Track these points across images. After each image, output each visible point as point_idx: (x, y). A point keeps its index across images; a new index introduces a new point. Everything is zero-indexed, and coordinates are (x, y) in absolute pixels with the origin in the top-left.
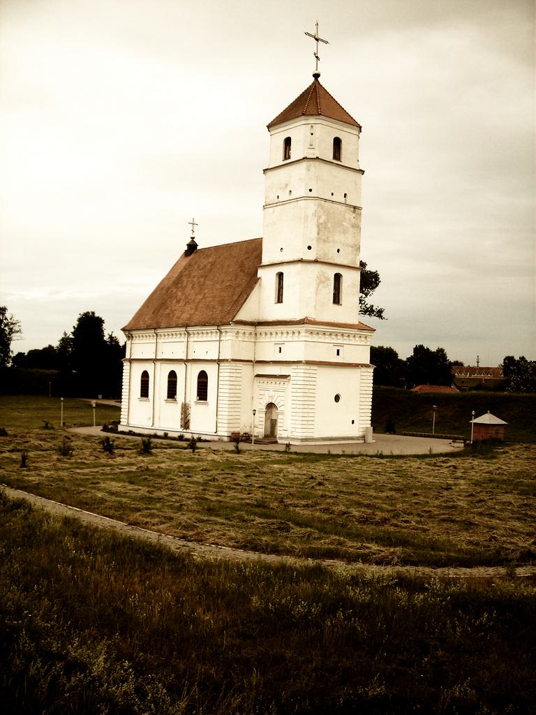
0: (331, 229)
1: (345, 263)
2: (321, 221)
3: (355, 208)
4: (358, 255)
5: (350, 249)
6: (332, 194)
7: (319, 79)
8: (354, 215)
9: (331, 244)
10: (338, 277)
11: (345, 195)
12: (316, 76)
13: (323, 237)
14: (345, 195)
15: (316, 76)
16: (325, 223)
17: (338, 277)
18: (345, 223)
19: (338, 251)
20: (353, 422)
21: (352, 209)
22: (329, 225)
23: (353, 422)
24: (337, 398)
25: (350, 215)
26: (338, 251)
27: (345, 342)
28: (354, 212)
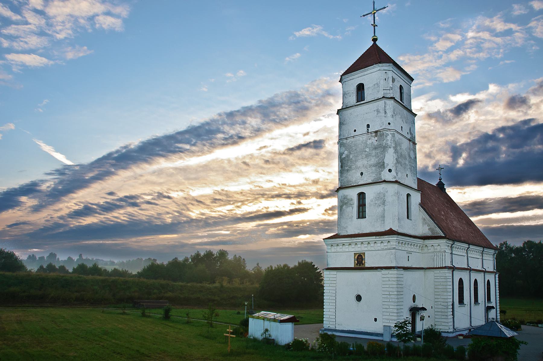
0: (354, 159)
1: (370, 181)
2: (344, 156)
3: (376, 132)
4: (382, 171)
5: (374, 168)
6: (355, 131)
7: (377, 42)
8: (376, 138)
9: (354, 171)
10: (362, 196)
11: (368, 126)
12: (375, 40)
13: (346, 168)
14: (368, 126)
15: (375, 40)
16: (348, 156)
17: (362, 196)
18: (367, 150)
19: (362, 174)
20: (376, 320)
21: (374, 134)
22: (351, 156)
23: (376, 320)
24: (359, 298)
25: (374, 140)
26: (362, 174)
27: (412, 250)
28: (376, 136)
